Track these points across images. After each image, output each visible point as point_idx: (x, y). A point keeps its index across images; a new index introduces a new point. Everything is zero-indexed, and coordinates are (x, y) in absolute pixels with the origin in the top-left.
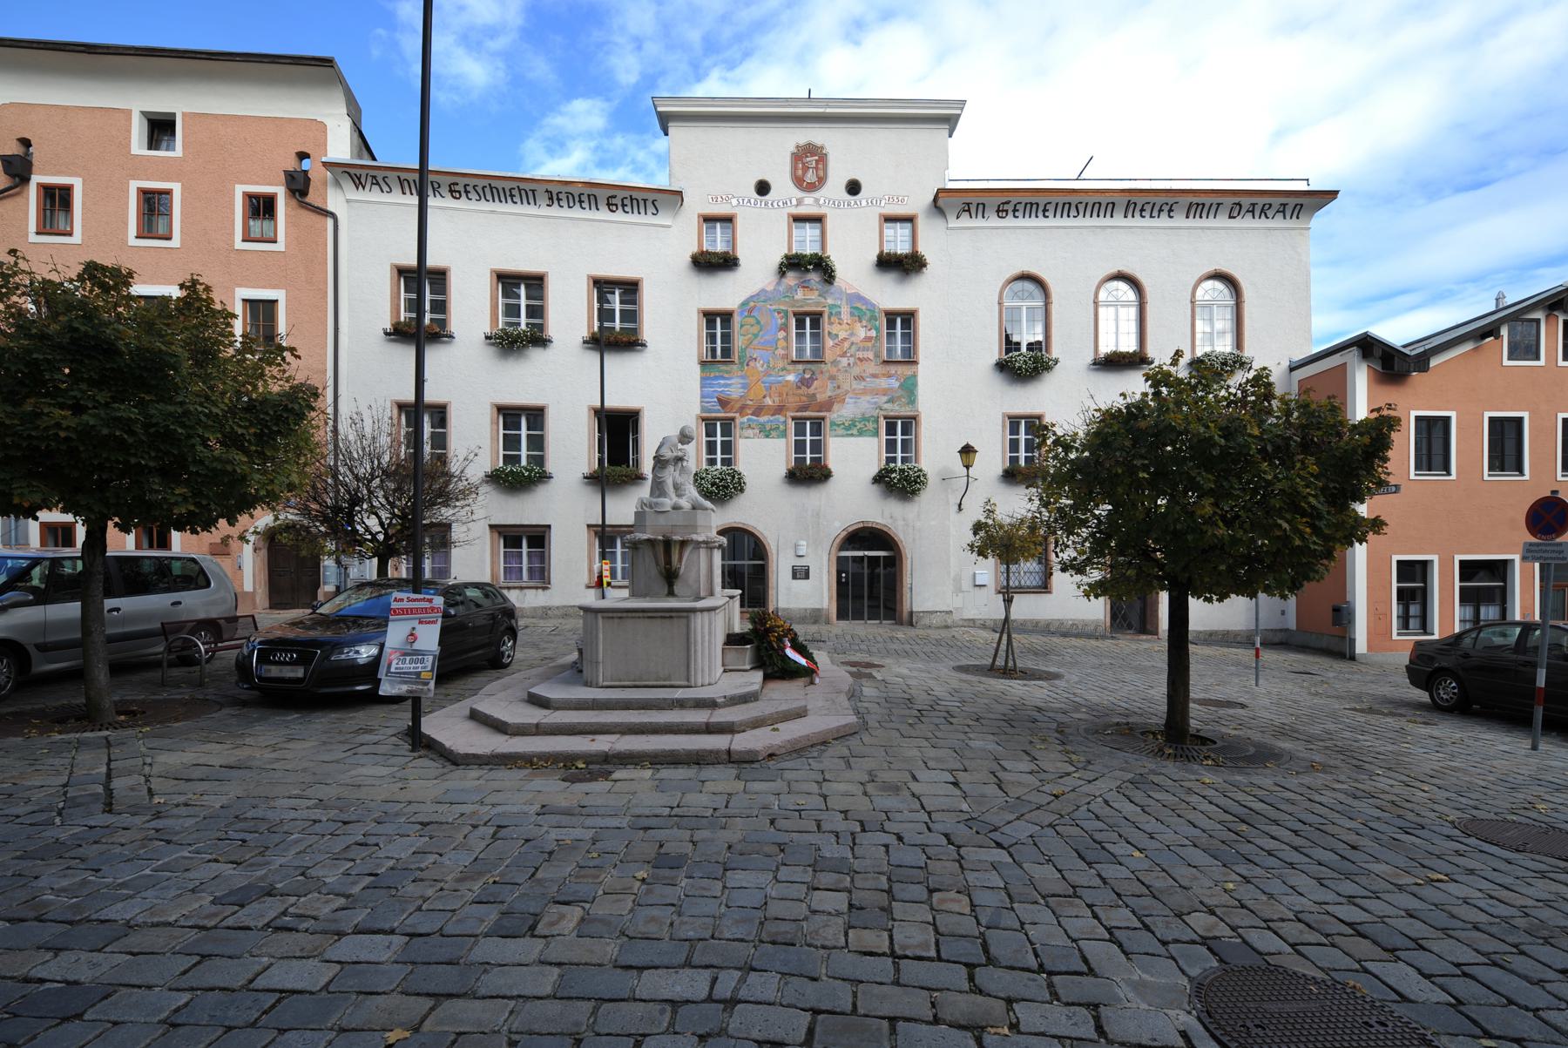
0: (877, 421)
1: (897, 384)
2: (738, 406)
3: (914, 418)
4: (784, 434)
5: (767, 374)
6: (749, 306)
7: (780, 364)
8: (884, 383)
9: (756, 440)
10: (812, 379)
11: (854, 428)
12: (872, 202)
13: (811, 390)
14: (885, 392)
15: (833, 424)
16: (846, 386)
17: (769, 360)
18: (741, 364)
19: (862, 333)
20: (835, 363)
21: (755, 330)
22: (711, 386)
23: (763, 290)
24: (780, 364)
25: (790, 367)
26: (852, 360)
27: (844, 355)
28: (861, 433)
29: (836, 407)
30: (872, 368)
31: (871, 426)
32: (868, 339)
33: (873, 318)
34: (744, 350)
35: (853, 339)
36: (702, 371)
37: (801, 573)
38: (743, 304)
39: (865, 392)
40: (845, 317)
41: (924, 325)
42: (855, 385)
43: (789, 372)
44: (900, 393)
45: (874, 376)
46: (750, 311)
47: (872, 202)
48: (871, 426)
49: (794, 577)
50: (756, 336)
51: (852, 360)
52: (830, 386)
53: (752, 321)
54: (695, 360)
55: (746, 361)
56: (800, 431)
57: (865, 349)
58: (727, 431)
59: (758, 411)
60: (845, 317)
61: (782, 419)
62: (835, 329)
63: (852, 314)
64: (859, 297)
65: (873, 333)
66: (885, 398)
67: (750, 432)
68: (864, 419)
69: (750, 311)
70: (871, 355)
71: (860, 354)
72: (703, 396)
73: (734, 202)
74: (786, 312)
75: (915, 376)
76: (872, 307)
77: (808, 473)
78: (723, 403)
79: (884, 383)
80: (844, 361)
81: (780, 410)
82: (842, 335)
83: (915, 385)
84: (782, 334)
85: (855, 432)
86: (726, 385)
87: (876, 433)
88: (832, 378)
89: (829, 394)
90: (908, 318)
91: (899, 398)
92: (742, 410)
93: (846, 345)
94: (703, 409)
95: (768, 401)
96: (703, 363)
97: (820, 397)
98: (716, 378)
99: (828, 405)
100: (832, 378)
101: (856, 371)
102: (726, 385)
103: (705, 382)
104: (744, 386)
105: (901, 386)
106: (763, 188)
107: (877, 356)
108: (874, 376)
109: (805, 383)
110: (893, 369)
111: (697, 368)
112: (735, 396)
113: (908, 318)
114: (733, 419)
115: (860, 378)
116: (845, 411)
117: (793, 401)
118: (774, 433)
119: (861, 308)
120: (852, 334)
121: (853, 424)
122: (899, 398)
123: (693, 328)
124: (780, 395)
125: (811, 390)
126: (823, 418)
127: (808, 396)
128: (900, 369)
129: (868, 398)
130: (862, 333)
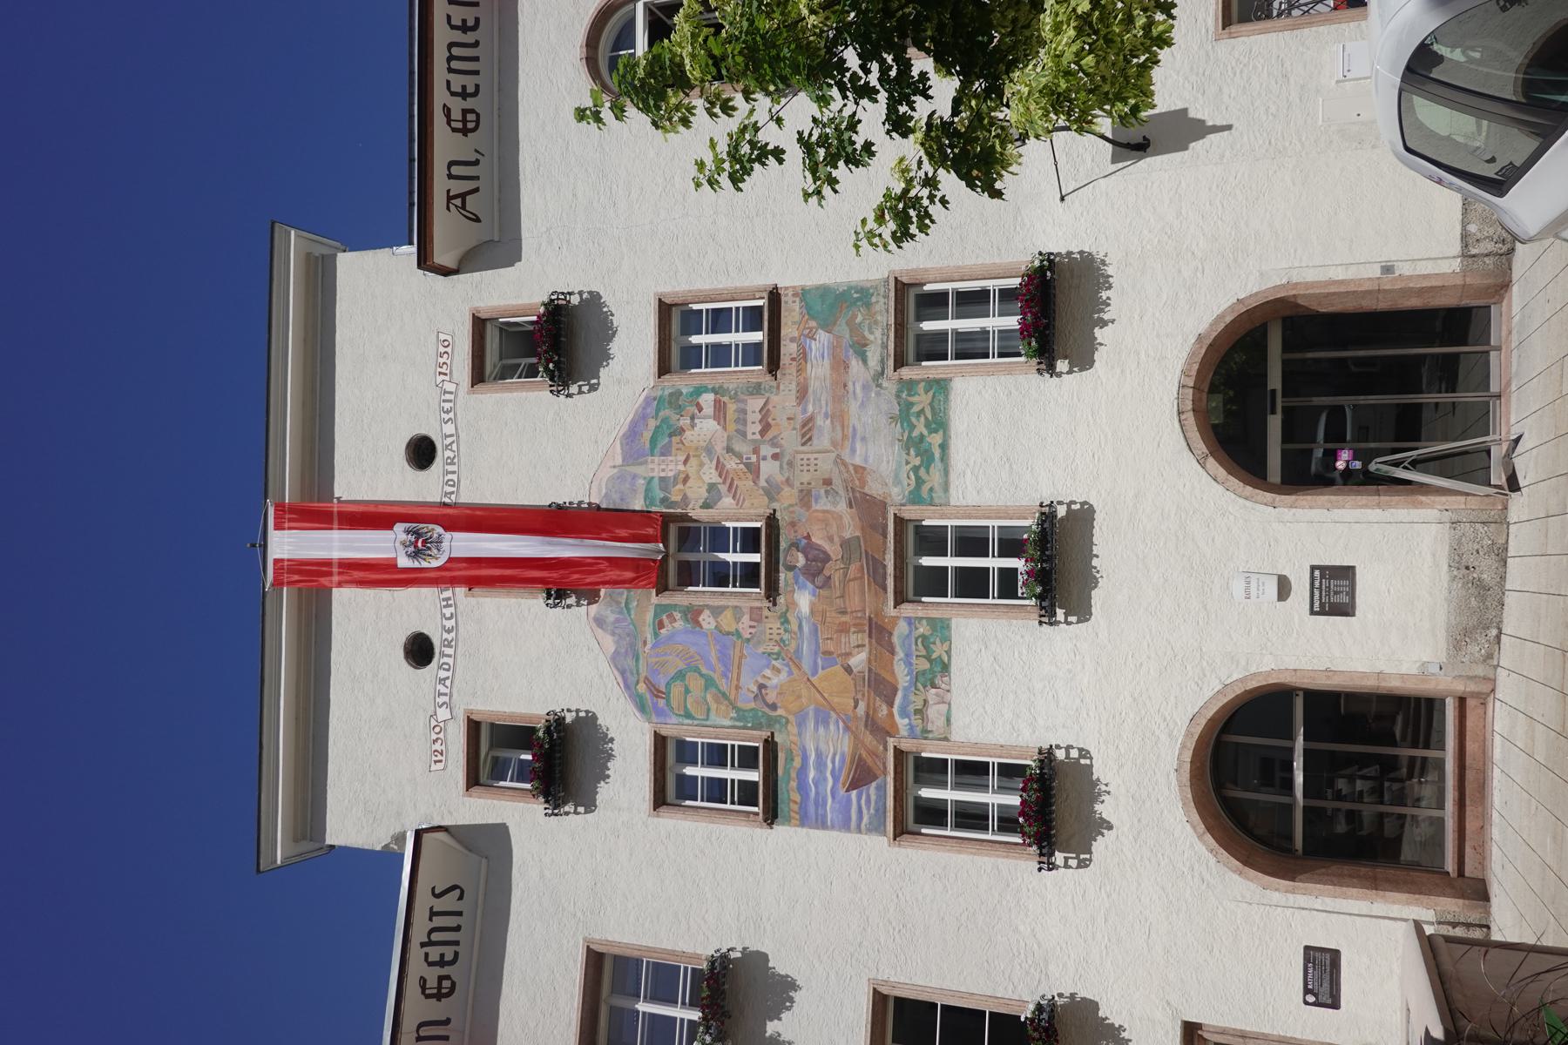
0: (910, 385)
1: (823, 336)
2: (869, 739)
3: (902, 288)
4: (941, 628)
5: (795, 660)
6: (649, 696)
7: (773, 625)
8: (819, 370)
9: (957, 697)
10: (808, 548)
11: (926, 436)
12: (449, 414)
13: (834, 550)
14: (840, 366)
15: (915, 498)
16: (826, 465)
17: (765, 657)
18: (771, 722)
19: (707, 427)
20: (771, 492)
21: (695, 683)
22: (820, 803)
23: (615, 659)
24: (773, 625)
25: (781, 600)
26: (766, 450)
27: (753, 470)
28: (939, 423)
29: (874, 489)
30: (783, 399)
31: (922, 399)
32: (720, 411)
33: (674, 401)
34: (741, 715)
35: (719, 448)
36: (788, 821)
37: (1334, 591)
38: (642, 707)
39: (839, 417)
40: (670, 467)
41: (677, 285)
42: (822, 440)
43: (792, 605)
44: (842, 329)
45: (802, 393)
46: (656, 693)
47: (449, 414)
48: (922, 399)
49: (1345, 610)
50: (709, 683)
51: (766, 450)
52: (823, 504)
53: (676, 690)
54: (761, 833)
55: (765, 710)
56: (934, 583)
57: (742, 420)
58: (932, 770)
59: (882, 687)
60: (670, 467)
61: (901, 628)
62: (697, 492)
63: (665, 452)
64: (632, 435)
65: (707, 399)
66: (855, 364)
67: (935, 712)
68: (904, 415)
69: (656, 693)
70: (755, 404)
71: (754, 429)
72: (845, 826)
73: (443, 714)
74: (660, 609)
75: (803, 294)
76: (655, 403)
77: (1050, 564)
78: (861, 776)
79: (819, 370)
80: (768, 468)
81: (879, 632)
82: (710, 475)
83: (824, 291)
84: (707, 620)
85: (936, 439)
86: (820, 764)
87: (941, 386)
88: (806, 497)
89: (842, 507)
90: (674, 318)
91: (854, 328)
92: (882, 731)
93: (731, 464)
94: (877, 828)
95: (859, 660)
96: (772, 816)
97: (851, 529)
98: (802, 788)
99: (868, 507)
100: (806, 497)
101: (790, 439)
102: (820, 764)
103: (811, 818)
104: (822, 720)
105: (827, 326)
106: (420, 651)
107: (756, 390)
108: (802, 393)
109: (816, 567)
110: (788, 349)
111: (780, 830)
112: (845, 744)
113: (674, 318)
114: (899, 754)
115: (807, 430)
116: (884, 463)
117: (859, 598)
118: (938, 651)
119: (655, 431)
120: (709, 450)
121: (915, 444)
122: (854, 328)
123: (689, 830)
124: (843, 629)
125: (834, 550)
126: (900, 522)
127: (847, 560)
128: (788, 330)
129: (853, 407)
130: (707, 427)
